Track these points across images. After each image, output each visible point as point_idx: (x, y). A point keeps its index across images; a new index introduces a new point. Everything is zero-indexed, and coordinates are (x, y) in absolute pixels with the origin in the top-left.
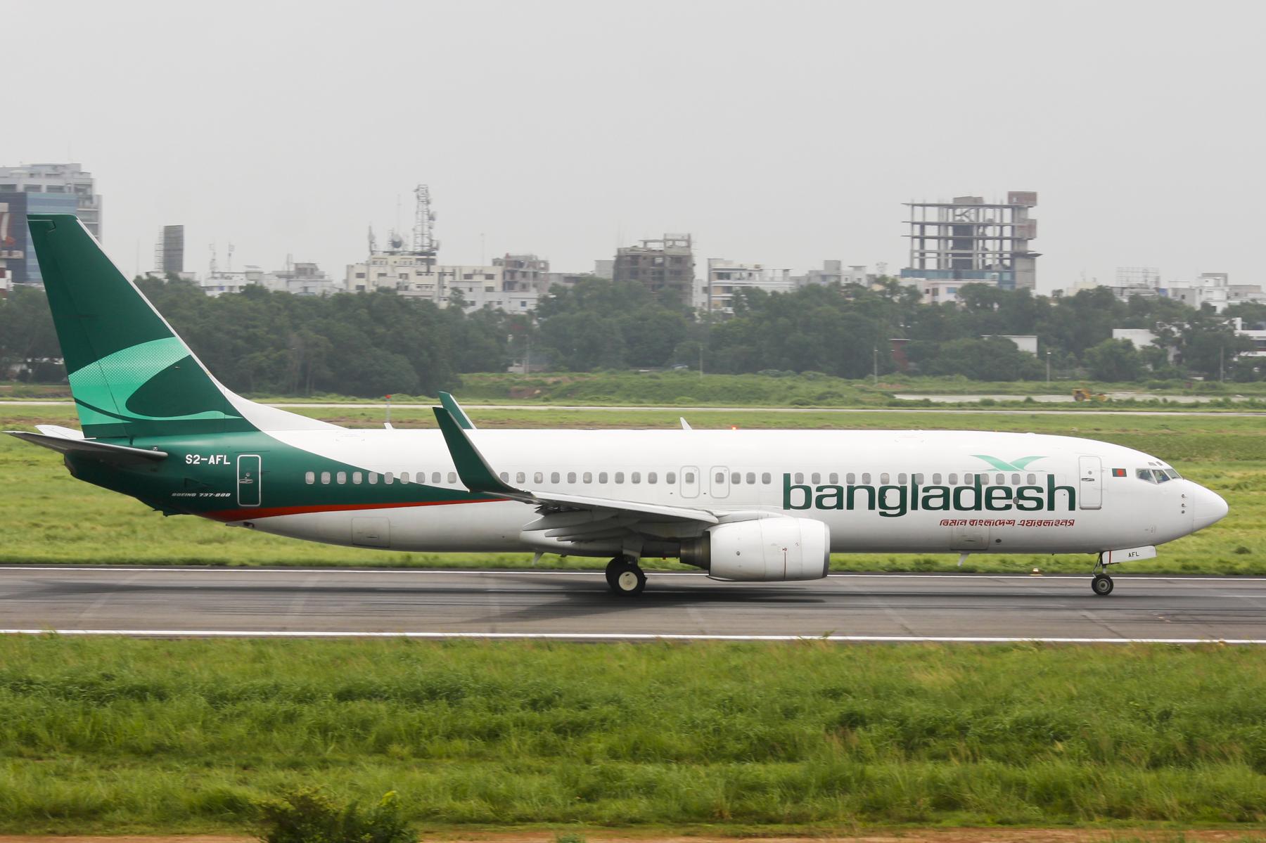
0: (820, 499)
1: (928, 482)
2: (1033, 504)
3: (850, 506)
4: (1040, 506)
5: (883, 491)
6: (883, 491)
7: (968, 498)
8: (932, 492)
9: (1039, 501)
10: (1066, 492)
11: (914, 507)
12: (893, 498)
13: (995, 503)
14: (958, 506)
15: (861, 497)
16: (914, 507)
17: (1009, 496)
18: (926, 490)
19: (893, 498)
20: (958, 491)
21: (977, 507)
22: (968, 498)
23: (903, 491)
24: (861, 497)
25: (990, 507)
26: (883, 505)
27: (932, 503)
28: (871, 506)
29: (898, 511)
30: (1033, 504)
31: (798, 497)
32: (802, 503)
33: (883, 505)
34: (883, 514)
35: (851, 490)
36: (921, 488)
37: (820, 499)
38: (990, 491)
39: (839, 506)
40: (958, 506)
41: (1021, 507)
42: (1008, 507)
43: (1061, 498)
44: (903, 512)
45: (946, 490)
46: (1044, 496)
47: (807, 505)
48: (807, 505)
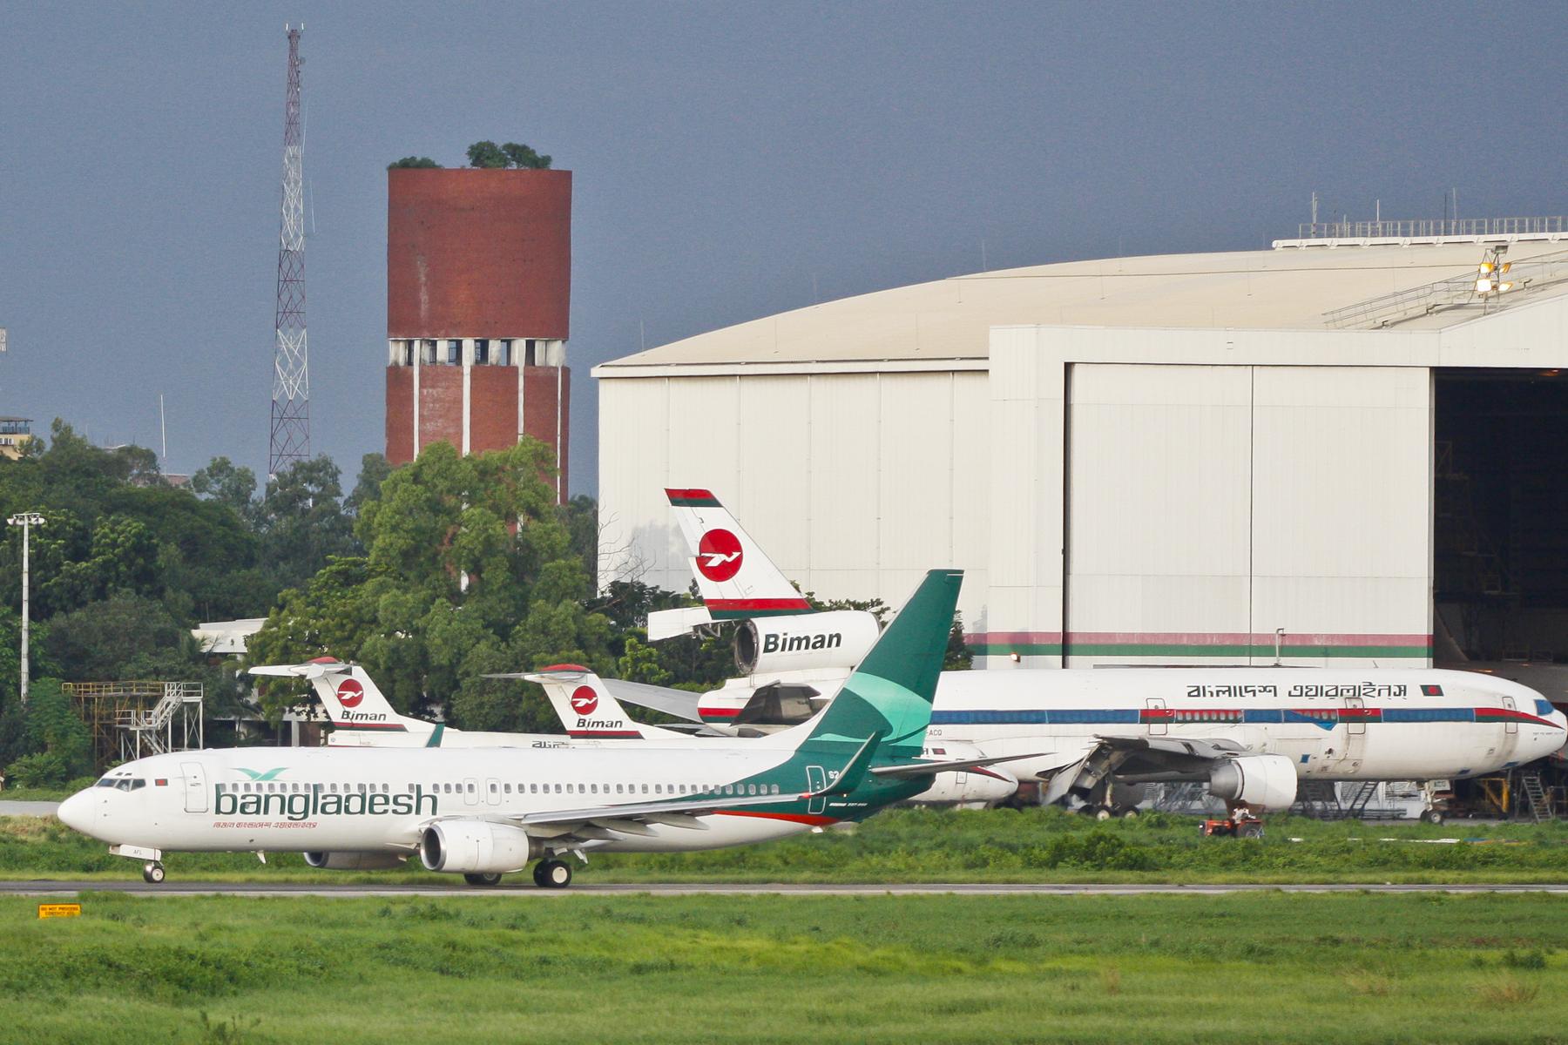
0: (243, 806)
1: (327, 791)
2: (405, 809)
3: (266, 812)
4: (409, 811)
5: (291, 798)
6: (291, 798)
7: (355, 804)
8: (329, 799)
9: (410, 807)
10: (430, 799)
11: (315, 812)
12: (299, 805)
13: (376, 808)
14: (347, 811)
15: (275, 803)
16: (315, 812)
17: (387, 802)
18: (324, 797)
19: (299, 805)
20: (348, 798)
21: (362, 812)
22: (355, 804)
23: (307, 798)
24: (275, 803)
25: (371, 811)
26: (291, 811)
27: (329, 808)
28: (282, 812)
29: (302, 815)
30: (405, 809)
31: (226, 804)
32: (230, 809)
33: (291, 811)
34: (290, 818)
35: (267, 798)
36: (320, 795)
37: (243, 806)
38: (372, 798)
39: (257, 812)
40: (347, 811)
41: (395, 812)
42: (385, 812)
43: (427, 803)
44: (306, 816)
45: (339, 798)
46: (413, 803)
47: (233, 811)
48: (233, 811)
